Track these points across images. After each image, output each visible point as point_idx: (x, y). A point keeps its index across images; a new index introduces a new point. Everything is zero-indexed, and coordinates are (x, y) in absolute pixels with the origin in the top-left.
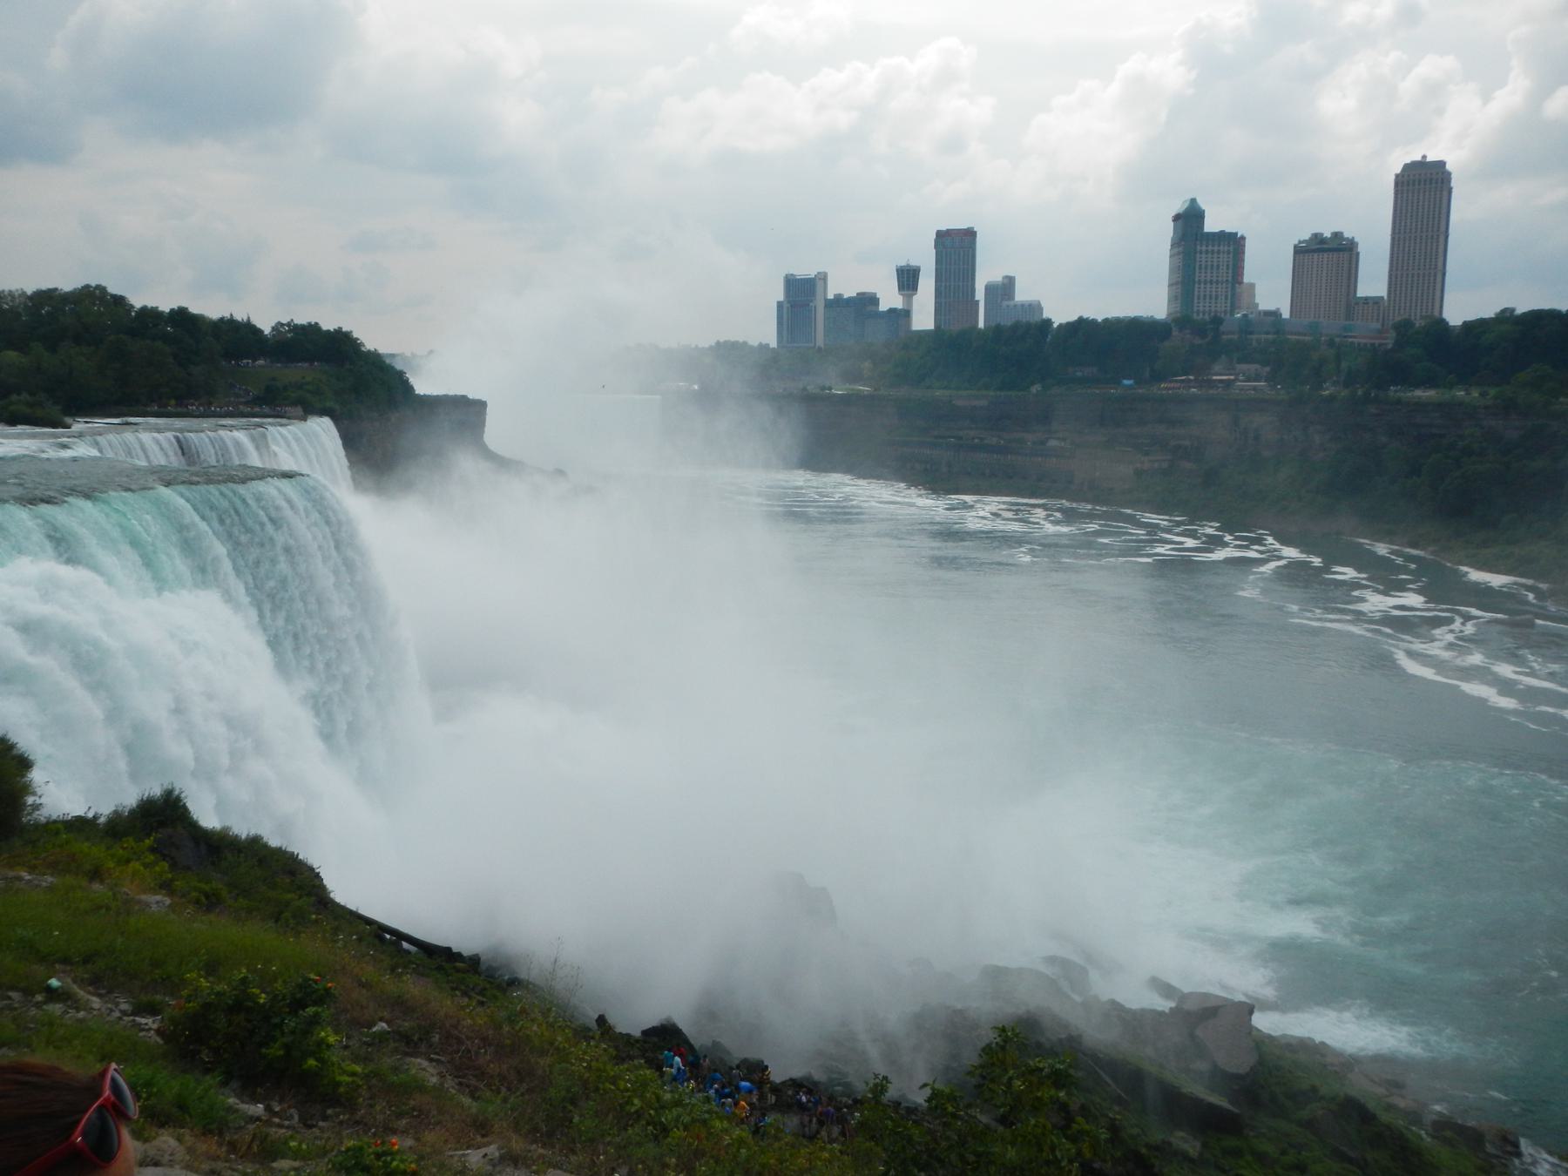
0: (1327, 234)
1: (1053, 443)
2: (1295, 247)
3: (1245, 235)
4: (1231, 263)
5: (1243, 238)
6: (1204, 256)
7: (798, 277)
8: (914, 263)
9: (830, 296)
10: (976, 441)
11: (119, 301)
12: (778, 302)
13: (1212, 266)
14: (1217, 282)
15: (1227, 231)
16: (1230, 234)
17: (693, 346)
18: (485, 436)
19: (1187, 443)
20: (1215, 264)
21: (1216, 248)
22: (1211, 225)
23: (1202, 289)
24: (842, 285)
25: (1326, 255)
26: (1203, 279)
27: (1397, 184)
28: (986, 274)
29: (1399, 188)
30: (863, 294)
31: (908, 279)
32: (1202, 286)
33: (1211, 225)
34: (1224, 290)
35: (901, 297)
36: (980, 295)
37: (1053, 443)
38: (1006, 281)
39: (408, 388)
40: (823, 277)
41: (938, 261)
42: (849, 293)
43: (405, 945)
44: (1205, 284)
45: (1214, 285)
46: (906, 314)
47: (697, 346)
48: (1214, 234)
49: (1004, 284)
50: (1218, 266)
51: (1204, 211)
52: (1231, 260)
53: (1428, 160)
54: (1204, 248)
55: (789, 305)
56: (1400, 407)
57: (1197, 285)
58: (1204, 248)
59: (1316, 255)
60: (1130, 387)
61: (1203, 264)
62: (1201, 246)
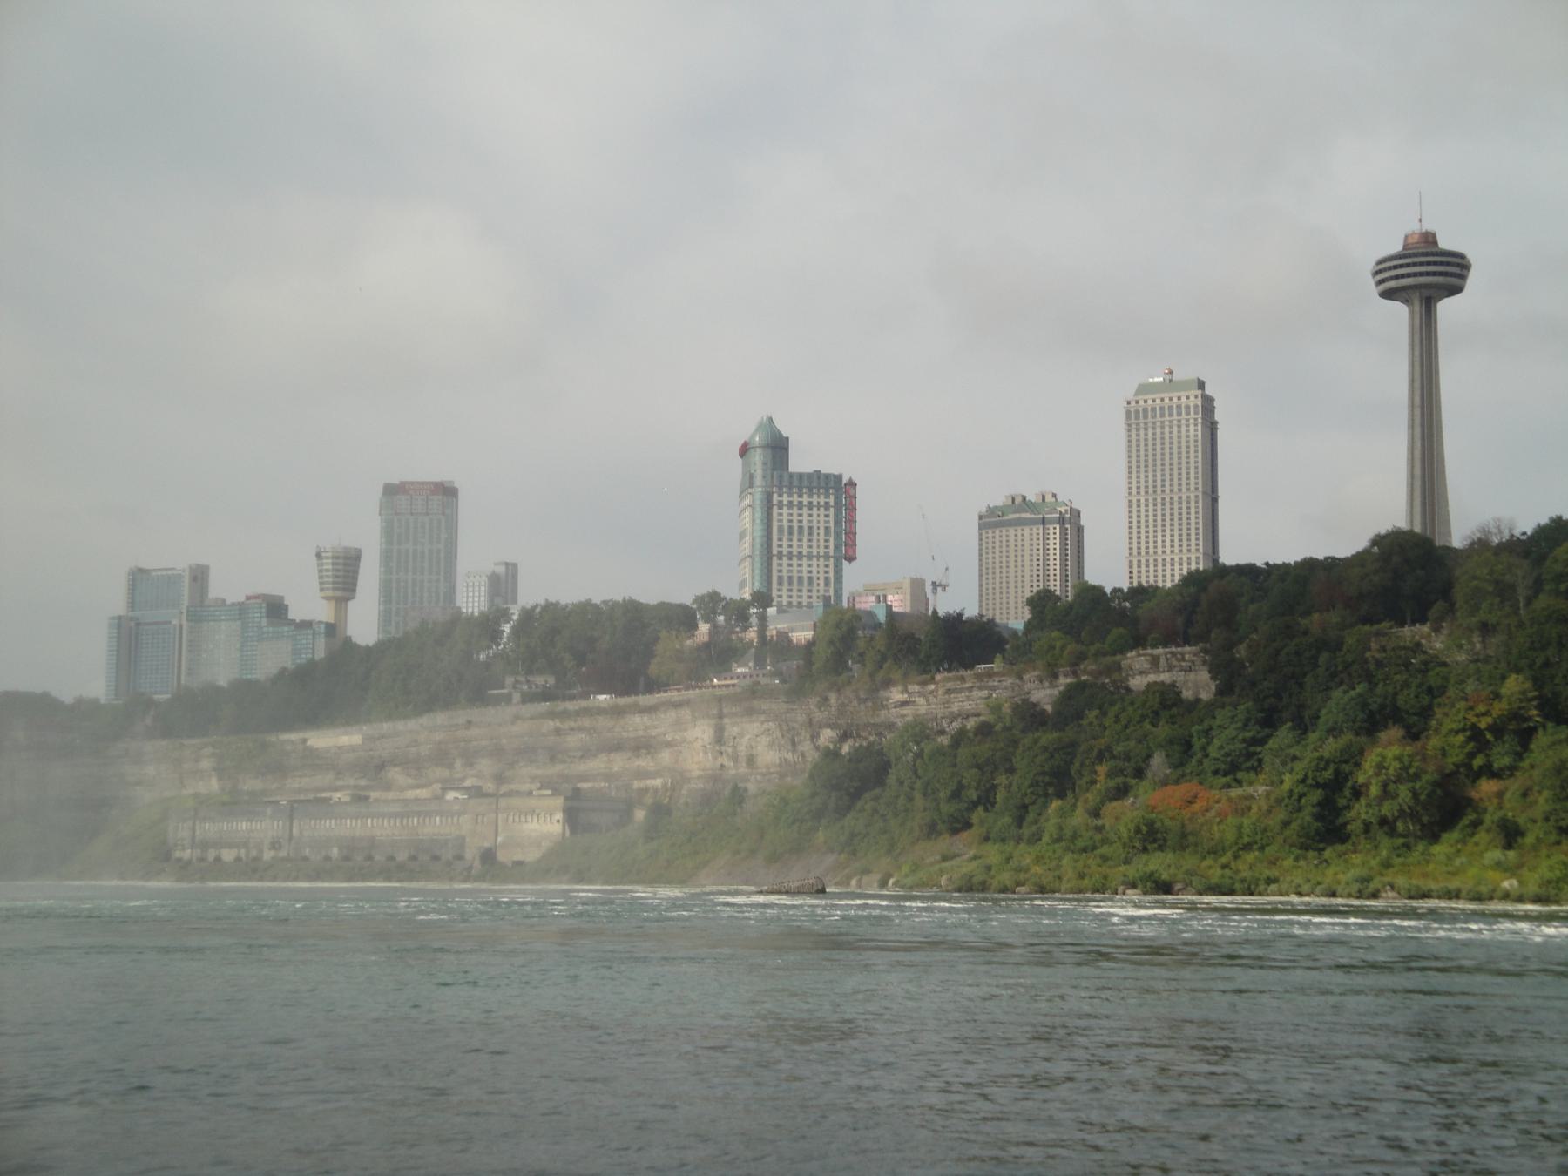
0: (1031, 497)
2: (980, 517)
3: (855, 480)
4: (832, 525)
5: (852, 484)
6: (785, 511)
7: (154, 574)
8: (350, 542)
13: (801, 528)
14: (810, 557)
15: (824, 471)
16: (827, 476)
19: (658, 782)
20: (805, 524)
21: (805, 500)
22: (799, 463)
23: (785, 568)
25: (1027, 531)
26: (785, 550)
27: (1128, 414)
29: (1133, 421)
30: (256, 597)
32: (785, 561)
33: (799, 463)
34: (822, 569)
35: (324, 602)
38: (501, 570)
40: (200, 576)
41: (388, 533)
42: (235, 596)
44: (790, 553)
45: (805, 561)
48: (801, 476)
50: (810, 528)
51: (787, 439)
52: (831, 519)
54: (785, 499)
55: (133, 624)
56: (932, 687)
57: (775, 561)
58: (785, 499)
59: (1012, 531)
61: (785, 524)
62: (780, 496)
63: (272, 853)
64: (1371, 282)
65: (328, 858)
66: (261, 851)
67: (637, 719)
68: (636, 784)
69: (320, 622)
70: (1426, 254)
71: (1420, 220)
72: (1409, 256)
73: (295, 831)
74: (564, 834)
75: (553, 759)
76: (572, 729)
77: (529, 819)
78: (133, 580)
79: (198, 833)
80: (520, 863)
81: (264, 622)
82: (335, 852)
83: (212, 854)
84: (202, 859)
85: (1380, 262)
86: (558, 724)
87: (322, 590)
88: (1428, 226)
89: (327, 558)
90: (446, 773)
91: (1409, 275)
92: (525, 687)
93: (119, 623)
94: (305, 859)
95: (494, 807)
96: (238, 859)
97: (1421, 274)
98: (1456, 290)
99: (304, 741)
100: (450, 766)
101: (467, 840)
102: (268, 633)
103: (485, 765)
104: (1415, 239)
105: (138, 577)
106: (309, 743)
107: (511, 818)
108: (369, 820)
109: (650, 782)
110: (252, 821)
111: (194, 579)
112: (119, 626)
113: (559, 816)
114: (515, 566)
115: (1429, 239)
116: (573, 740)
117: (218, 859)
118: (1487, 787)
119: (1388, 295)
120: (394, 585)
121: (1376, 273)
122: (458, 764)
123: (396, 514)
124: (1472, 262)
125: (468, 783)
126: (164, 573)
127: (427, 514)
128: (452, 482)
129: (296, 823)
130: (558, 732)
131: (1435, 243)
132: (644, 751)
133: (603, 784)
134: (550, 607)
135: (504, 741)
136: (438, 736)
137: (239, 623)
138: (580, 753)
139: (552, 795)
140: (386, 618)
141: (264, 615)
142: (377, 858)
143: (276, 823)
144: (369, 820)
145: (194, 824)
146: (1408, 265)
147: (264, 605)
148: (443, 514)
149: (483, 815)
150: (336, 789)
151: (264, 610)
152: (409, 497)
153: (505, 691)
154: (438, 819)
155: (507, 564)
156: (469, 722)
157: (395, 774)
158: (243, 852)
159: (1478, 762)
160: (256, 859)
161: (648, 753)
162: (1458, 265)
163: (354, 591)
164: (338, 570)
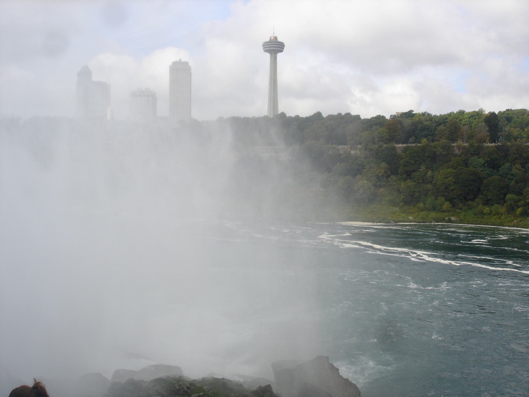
53: (182, 61)
64: (262, 48)
70: (274, 42)
71: (274, 33)
72: (270, 42)
85: (264, 43)
88: (275, 35)
91: (273, 47)
97: (276, 47)
98: (282, 51)
104: (272, 38)
115: (276, 38)
118: (381, 190)
119: (266, 51)
121: (263, 46)
124: (285, 44)
131: (277, 40)
146: (271, 44)
159: (378, 184)
162: (282, 45)
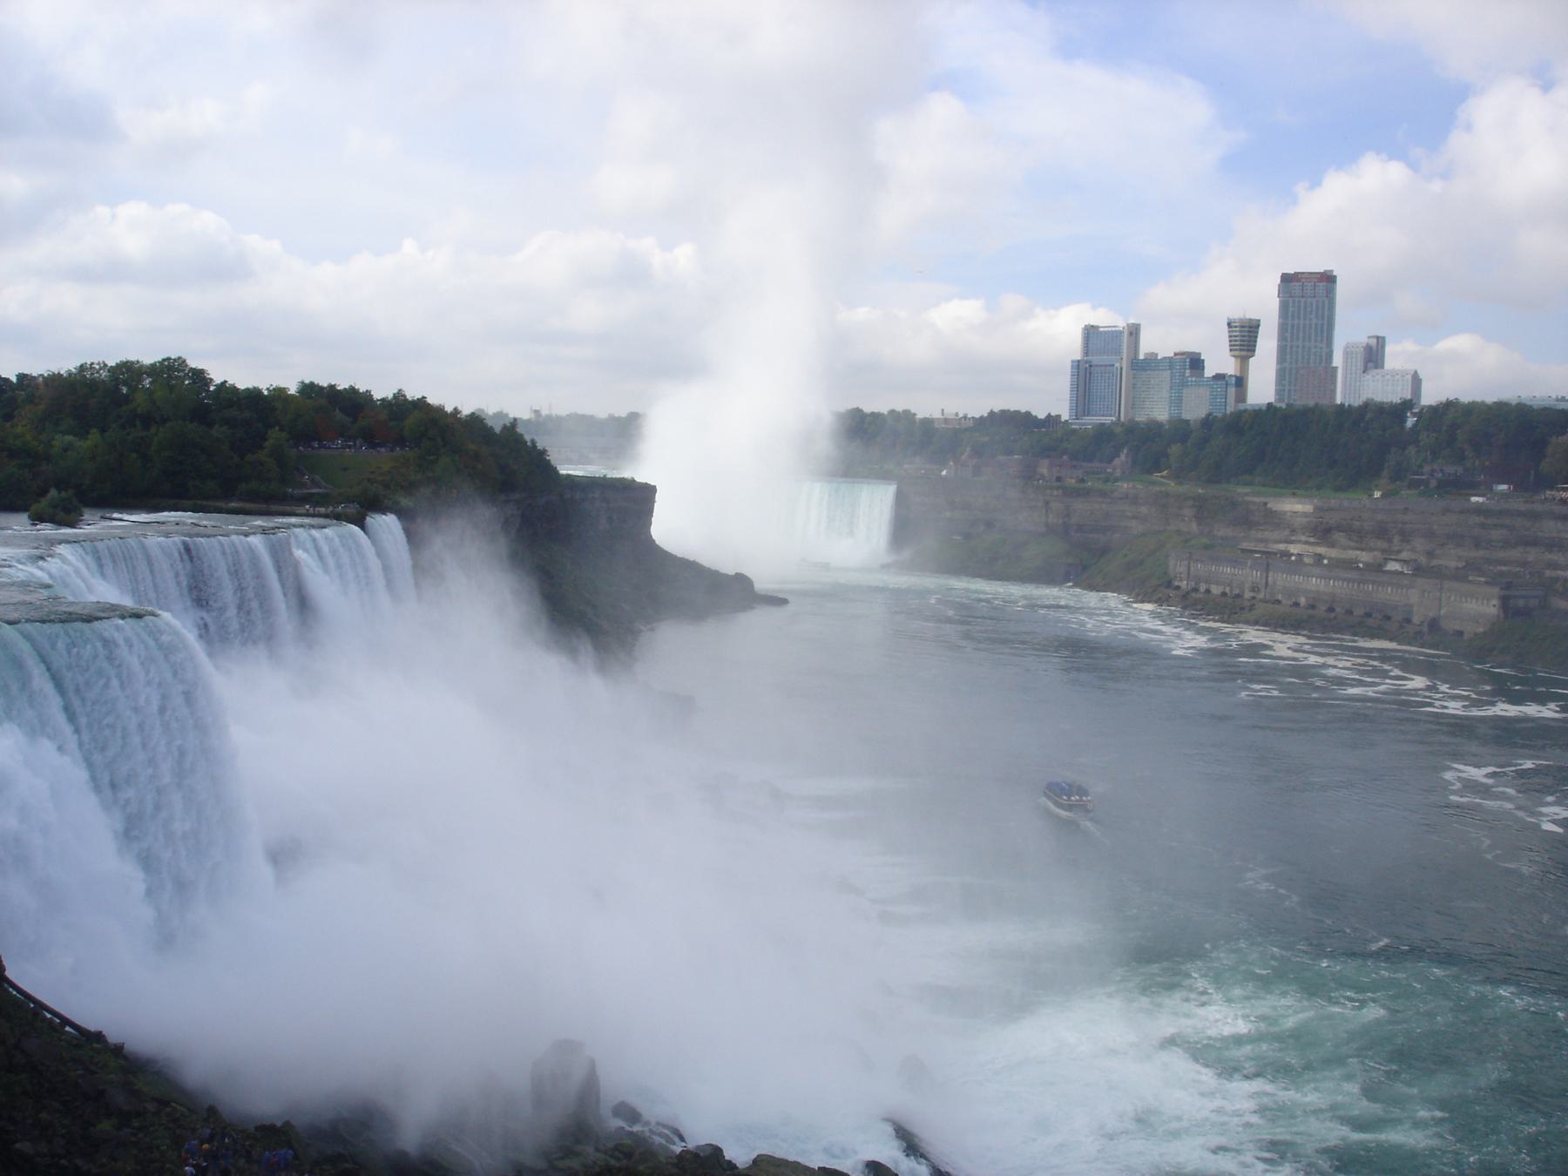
1: (1393, 566)
7: (1101, 329)
8: (1253, 317)
9: (1141, 357)
10: (1293, 558)
11: (199, 376)
12: (1072, 361)
17: (961, 415)
18: (652, 527)
24: (1158, 342)
28: (1348, 332)
31: (1244, 336)
35: (1233, 359)
36: (1338, 360)
37: (1393, 566)
38: (1373, 342)
39: (548, 470)
40: (1134, 331)
43: (67, 1028)
46: (1241, 382)
47: (965, 417)
49: (1368, 344)
55: (1087, 365)
60: (1503, 495)
63: (1252, 594)
65: (1296, 604)
66: (1243, 592)
67: (1551, 523)
68: (1548, 573)
69: (1231, 375)
73: (1270, 579)
74: (1498, 616)
75: (1477, 545)
76: (1496, 525)
77: (1469, 600)
78: (1088, 337)
79: (1192, 569)
80: (1460, 633)
81: (1188, 372)
82: (1303, 601)
83: (1203, 587)
84: (1196, 590)
86: (1482, 519)
87: (1231, 350)
89: (1236, 327)
90: (1385, 545)
92: (1440, 474)
93: (1077, 365)
94: (1278, 602)
95: (1439, 586)
96: (1224, 594)
99: (1266, 504)
100: (1390, 541)
101: (1415, 609)
102: (1192, 382)
103: (1420, 544)
105: (1090, 332)
106: (1269, 506)
107: (1452, 599)
108: (1331, 582)
109: (1560, 573)
110: (1235, 568)
111: (1131, 334)
112: (1078, 365)
113: (1495, 602)
114: (1383, 338)
116: (1496, 534)
117: (1208, 591)
120: (1288, 350)
122: (1396, 539)
123: (1291, 297)
125: (1404, 555)
126: (1110, 329)
127: (1314, 297)
128: (1332, 271)
129: (1271, 574)
130: (1483, 526)
132: (1556, 549)
133: (1518, 569)
134: (1449, 405)
135: (1435, 527)
136: (1380, 517)
137: (1169, 371)
138: (1501, 544)
139: (1487, 583)
140: (1281, 375)
141: (1187, 367)
142: (1338, 610)
143: (1255, 572)
144: (1331, 582)
145: (1189, 564)
147: (1188, 360)
148: (1327, 296)
149: (1429, 593)
150: (1291, 542)
151: (1188, 364)
152: (1301, 284)
153: (1423, 477)
154: (1389, 589)
155: (1378, 338)
156: (1406, 509)
157: (1339, 537)
158: (1227, 590)
160: (1238, 596)
161: (1559, 551)
163: (1254, 351)
164: (1243, 336)
